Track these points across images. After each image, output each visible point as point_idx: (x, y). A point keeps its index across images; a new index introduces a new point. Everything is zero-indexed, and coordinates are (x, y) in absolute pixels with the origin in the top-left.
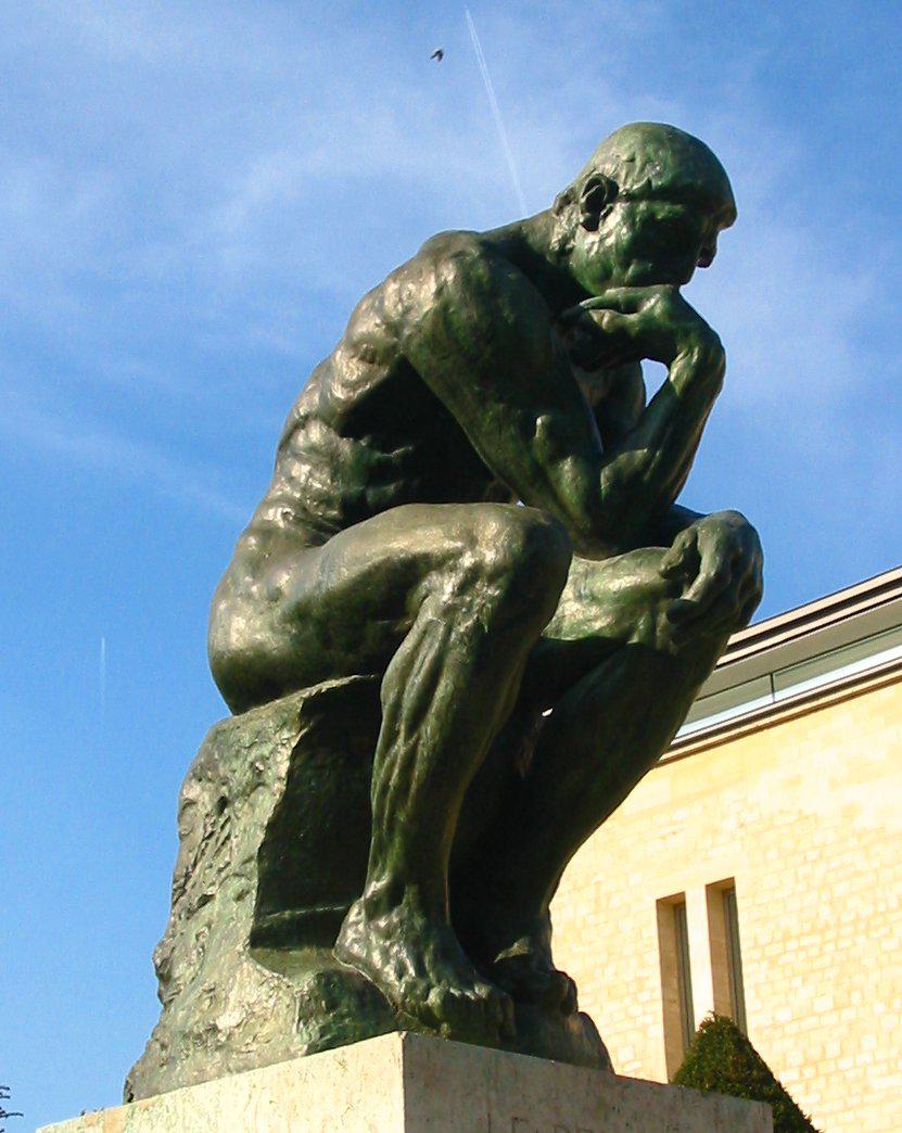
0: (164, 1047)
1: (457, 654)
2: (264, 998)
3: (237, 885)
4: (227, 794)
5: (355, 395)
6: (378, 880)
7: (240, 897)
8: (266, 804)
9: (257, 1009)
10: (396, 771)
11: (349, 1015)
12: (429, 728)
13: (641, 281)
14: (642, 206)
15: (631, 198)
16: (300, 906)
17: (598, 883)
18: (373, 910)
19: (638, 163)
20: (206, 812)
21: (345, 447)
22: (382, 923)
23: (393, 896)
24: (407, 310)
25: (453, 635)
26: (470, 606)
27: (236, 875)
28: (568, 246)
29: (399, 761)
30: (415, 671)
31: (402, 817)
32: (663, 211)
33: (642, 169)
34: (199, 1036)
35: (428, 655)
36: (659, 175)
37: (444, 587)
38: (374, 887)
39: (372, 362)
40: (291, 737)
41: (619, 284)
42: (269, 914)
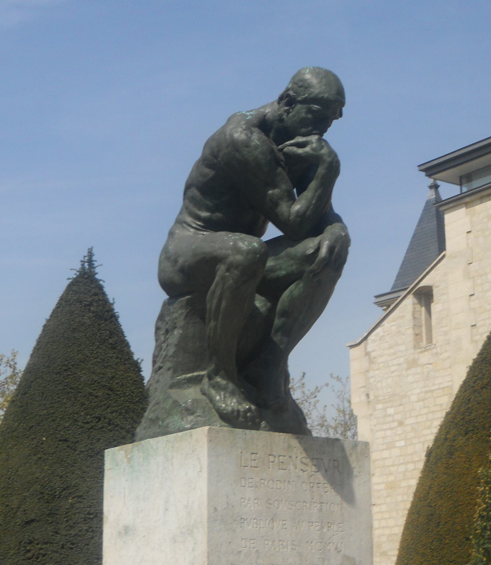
3: (168, 365)
7: (169, 369)
14: (305, 106)
18: (210, 378)
24: (219, 151)
27: (169, 361)
35: (218, 292)
37: (221, 269)
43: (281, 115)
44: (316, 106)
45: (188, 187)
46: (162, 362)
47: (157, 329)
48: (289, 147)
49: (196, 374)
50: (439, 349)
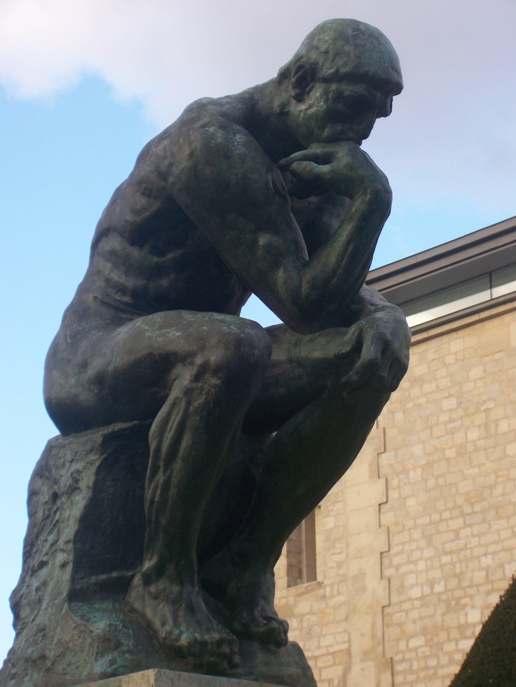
0: (13, 665)
1: (194, 421)
2: (76, 638)
3: (61, 557)
4: (57, 491)
5: (139, 219)
6: (150, 559)
7: (63, 566)
8: (80, 502)
9: (71, 645)
10: (159, 492)
11: (128, 651)
12: (178, 466)
13: (333, 140)
14: (334, 87)
15: (326, 80)
16: (103, 573)
17: (487, 410)
18: (147, 580)
19: (331, 55)
20: (44, 501)
21: (135, 253)
22: (153, 589)
23: (159, 571)
24: (171, 165)
25: (191, 408)
26: (201, 389)
27: (62, 550)
28: (285, 110)
29: (160, 486)
30: (168, 429)
31: (163, 521)
32: (348, 89)
33: (333, 60)
34: (34, 661)
36: (345, 65)
37: (183, 377)
38: (148, 565)
39: (149, 196)
40: (96, 459)
41: (320, 141)
42: (82, 578)
43: (284, 106)
44: (351, 88)
45: (102, 234)
46: (47, 554)
47: (33, 494)
48: (301, 163)
49: (114, 574)
50: (328, 590)
